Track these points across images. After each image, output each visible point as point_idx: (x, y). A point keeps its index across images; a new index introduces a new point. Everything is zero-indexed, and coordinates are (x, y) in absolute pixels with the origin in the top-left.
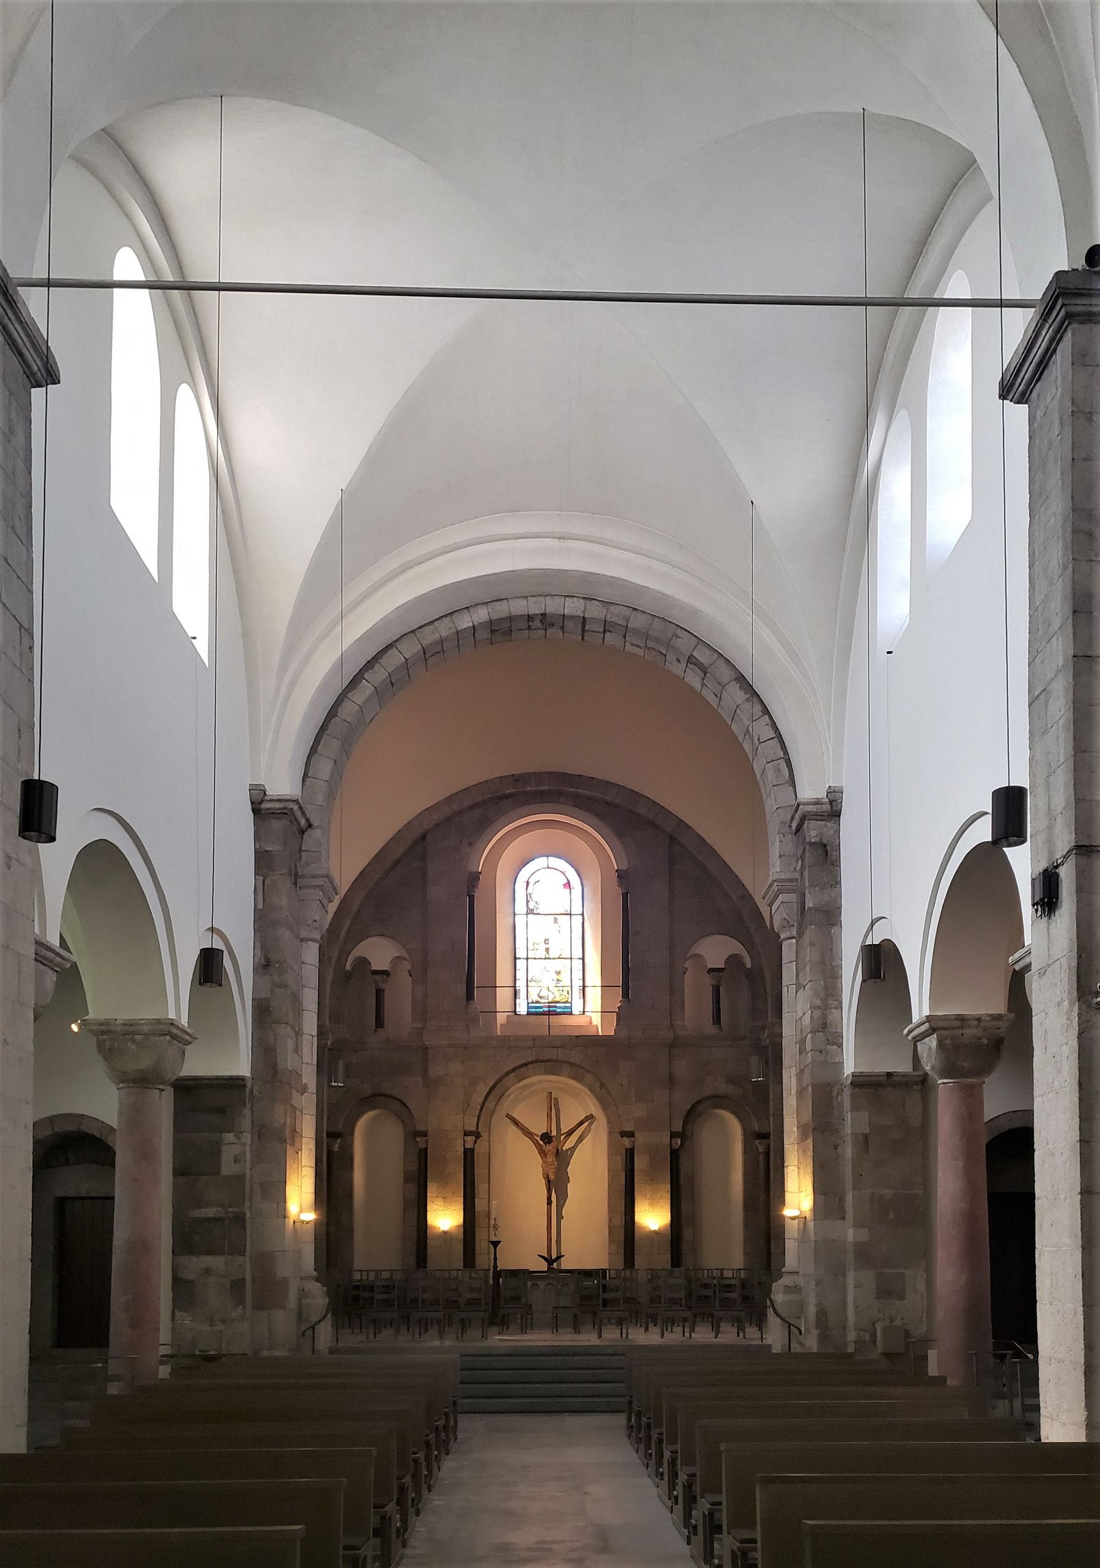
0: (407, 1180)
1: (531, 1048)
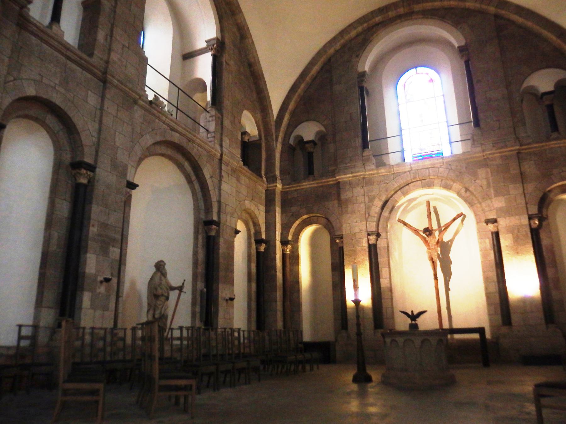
1: (409, 171)
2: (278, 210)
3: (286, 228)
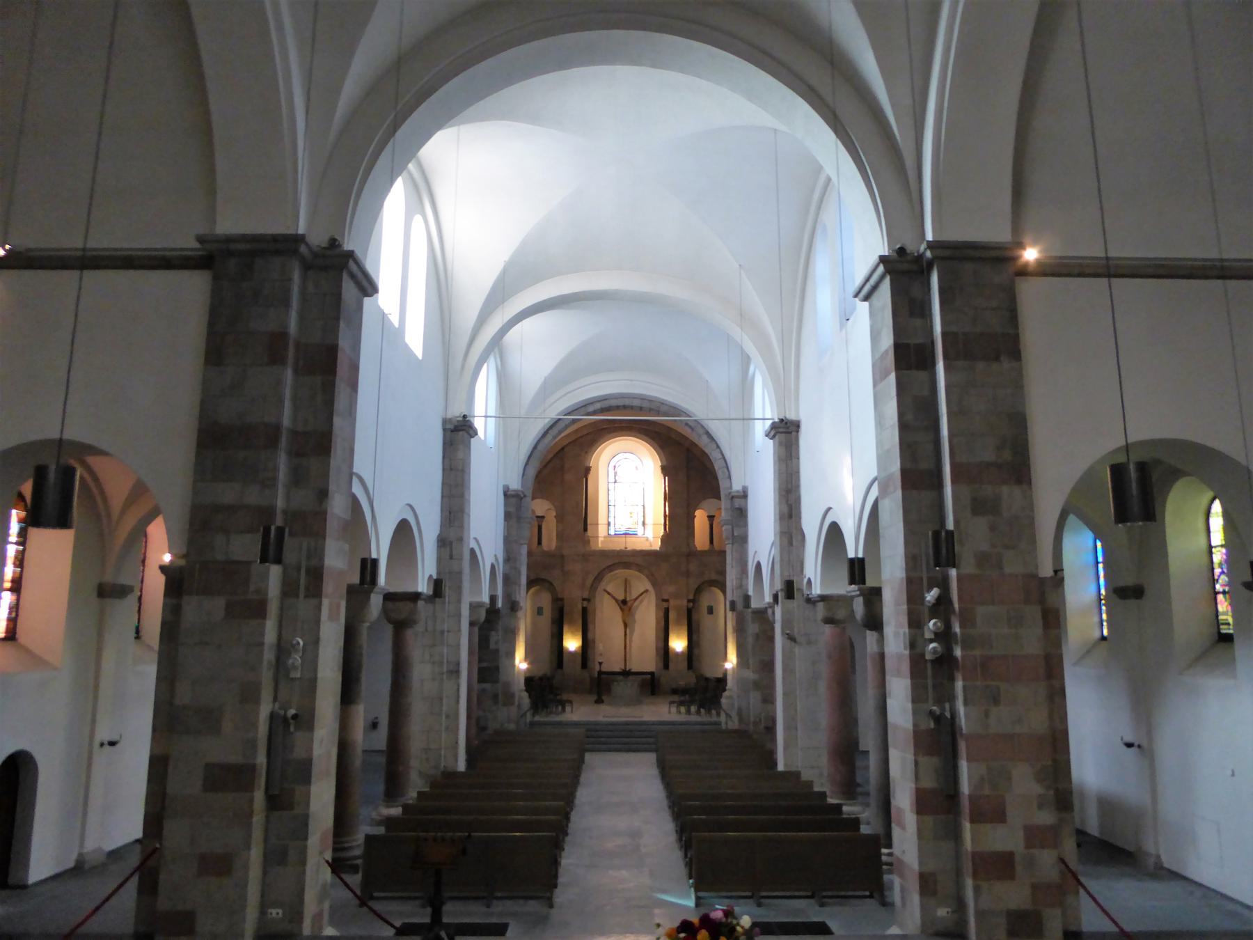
0: (553, 622)
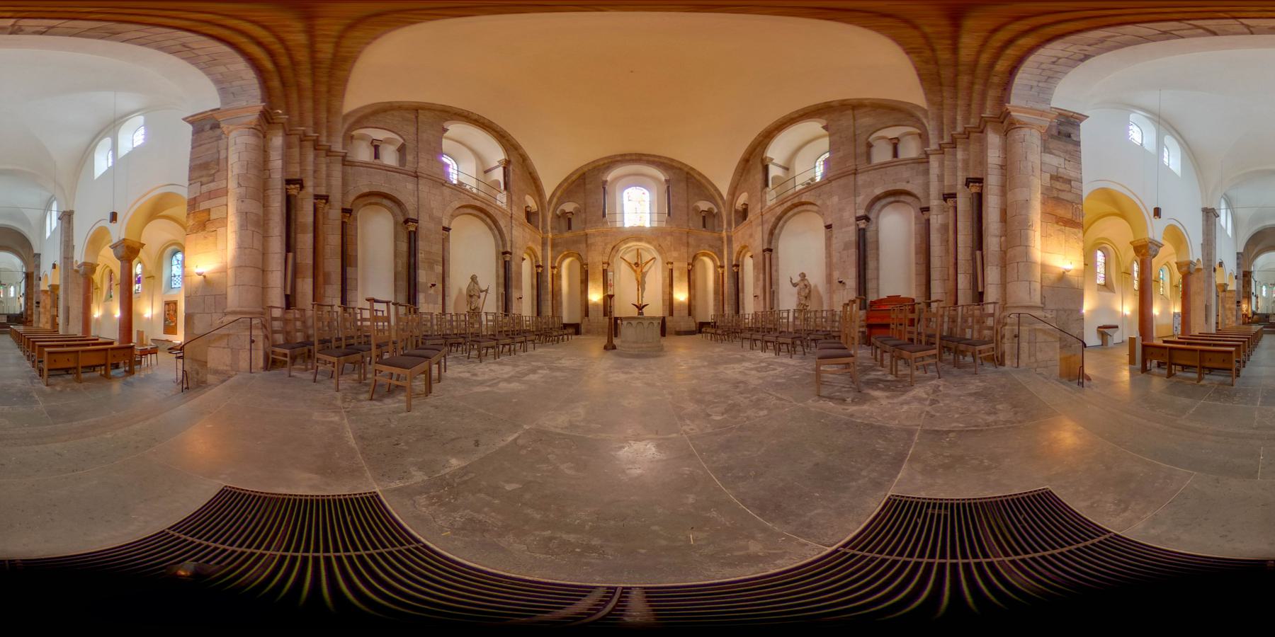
0: (582, 282)
2: (549, 249)
3: (554, 259)
